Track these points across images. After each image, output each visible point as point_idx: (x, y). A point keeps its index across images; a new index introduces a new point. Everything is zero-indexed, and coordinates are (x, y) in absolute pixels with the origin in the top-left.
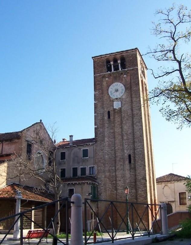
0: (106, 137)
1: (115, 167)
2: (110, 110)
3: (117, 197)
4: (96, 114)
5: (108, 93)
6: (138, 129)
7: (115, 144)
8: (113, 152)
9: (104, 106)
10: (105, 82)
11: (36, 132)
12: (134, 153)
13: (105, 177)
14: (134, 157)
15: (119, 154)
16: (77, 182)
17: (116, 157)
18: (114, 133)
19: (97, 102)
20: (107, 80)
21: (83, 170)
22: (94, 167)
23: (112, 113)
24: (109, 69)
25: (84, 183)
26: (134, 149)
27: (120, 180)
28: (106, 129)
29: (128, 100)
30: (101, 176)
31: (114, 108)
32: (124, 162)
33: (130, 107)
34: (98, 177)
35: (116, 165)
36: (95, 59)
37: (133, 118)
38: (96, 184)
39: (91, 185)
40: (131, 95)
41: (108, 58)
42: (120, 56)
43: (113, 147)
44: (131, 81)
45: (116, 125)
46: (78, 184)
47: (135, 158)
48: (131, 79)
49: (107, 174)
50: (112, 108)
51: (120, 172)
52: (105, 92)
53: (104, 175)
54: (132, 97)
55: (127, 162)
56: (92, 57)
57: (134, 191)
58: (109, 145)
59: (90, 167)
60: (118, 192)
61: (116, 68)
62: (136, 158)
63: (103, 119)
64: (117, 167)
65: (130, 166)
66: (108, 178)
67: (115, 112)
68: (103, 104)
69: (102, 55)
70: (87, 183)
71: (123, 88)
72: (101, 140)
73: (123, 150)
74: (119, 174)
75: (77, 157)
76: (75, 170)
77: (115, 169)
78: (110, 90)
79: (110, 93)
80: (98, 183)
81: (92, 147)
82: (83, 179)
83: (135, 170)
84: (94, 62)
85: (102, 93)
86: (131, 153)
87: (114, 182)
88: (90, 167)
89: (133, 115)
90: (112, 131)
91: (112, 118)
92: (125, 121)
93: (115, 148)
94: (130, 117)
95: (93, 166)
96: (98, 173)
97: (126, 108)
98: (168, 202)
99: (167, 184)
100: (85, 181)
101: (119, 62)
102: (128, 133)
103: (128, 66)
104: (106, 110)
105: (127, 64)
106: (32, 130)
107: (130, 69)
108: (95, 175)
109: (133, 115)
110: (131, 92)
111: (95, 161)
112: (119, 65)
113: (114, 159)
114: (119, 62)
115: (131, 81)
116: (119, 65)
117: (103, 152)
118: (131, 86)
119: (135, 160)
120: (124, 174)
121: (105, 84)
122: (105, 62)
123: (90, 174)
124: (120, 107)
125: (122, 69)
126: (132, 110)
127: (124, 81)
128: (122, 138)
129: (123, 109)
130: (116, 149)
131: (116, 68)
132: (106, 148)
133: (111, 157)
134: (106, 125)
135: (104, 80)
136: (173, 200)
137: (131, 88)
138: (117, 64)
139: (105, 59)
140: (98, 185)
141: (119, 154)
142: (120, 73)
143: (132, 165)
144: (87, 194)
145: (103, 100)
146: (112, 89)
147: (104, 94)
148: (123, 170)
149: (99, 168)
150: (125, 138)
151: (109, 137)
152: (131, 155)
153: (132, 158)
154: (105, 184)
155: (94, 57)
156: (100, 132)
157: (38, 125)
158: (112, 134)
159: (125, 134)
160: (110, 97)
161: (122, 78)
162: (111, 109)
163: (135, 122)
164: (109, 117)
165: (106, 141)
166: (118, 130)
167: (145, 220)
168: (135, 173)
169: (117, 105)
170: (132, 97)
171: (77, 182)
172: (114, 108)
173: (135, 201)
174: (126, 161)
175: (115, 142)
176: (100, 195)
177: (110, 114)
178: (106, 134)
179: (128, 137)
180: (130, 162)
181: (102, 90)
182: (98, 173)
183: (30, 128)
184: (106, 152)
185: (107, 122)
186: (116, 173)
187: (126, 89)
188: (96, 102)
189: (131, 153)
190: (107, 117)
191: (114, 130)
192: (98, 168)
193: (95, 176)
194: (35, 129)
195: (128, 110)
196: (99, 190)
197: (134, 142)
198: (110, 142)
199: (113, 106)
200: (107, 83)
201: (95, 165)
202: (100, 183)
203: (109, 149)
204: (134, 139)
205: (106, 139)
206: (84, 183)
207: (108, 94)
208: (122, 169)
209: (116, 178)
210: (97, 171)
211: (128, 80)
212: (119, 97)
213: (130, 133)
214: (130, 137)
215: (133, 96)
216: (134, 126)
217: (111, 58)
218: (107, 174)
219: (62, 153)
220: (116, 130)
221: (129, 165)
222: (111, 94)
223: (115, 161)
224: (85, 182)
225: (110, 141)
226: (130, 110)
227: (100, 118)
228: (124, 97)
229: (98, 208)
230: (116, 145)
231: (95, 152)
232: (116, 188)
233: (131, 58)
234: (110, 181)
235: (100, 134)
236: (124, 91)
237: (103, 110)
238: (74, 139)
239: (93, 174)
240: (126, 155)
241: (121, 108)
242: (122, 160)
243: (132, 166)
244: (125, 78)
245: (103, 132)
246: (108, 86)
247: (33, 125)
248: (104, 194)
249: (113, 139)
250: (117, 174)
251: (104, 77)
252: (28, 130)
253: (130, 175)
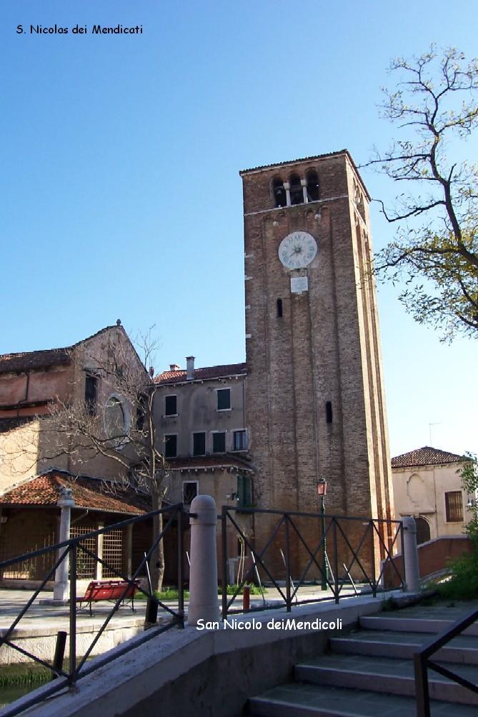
0: (272, 360)
1: (295, 431)
2: (282, 297)
3: (298, 503)
4: (249, 307)
5: (277, 256)
6: (349, 342)
7: (293, 378)
8: (290, 396)
9: (269, 286)
10: (271, 231)
11: (106, 349)
12: (340, 398)
13: (271, 455)
14: (340, 409)
15: (303, 401)
16: (204, 467)
17: (295, 408)
18: (292, 350)
19: (251, 278)
20: (276, 227)
21: (219, 439)
22: (245, 431)
23: (286, 304)
24: (280, 200)
25: (221, 470)
26: (340, 390)
27: (305, 464)
28: (273, 343)
29: (324, 272)
30: (262, 453)
31: (292, 291)
32: (315, 421)
33: (329, 290)
34: (255, 454)
35: (297, 427)
37: (336, 316)
38: (249, 472)
39: (237, 475)
40: (333, 262)
41: (276, 174)
42: (306, 170)
43: (290, 386)
44: (331, 228)
45: (297, 331)
46: (206, 473)
47: (340, 410)
48: (331, 224)
49: (276, 448)
50: (287, 291)
51: (306, 444)
52: (271, 255)
53: (269, 451)
54: (333, 267)
55: (322, 420)
56: (241, 173)
57: (340, 487)
58: (280, 380)
59: (235, 433)
60: (302, 490)
61: (297, 199)
62: (344, 411)
63: (266, 318)
64: (299, 432)
65: (330, 430)
66: (278, 458)
67: (293, 303)
68: (266, 283)
69: (262, 167)
70: (228, 469)
71: (314, 244)
72: (261, 368)
73: (312, 392)
74: (303, 447)
75: (204, 407)
76: (200, 438)
77: (295, 438)
78: (282, 249)
79: (281, 258)
80: (255, 471)
81: (240, 384)
82: (217, 459)
83: (342, 439)
84: (245, 183)
85: (264, 257)
86: (333, 397)
87: (293, 467)
88: (235, 433)
89: (336, 307)
90: (287, 347)
91: (286, 315)
93: (293, 387)
94: (330, 312)
95: (242, 429)
96: (255, 445)
97: (321, 291)
98: (420, 514)
99: (418, 471)
100: (224, 466)
101: (303, 182)
102: (324, 352)
103: (326, 194)
104: (273, 297)
105: (323, 188)
106: (97, 343)
108: (247, 451)
109: (336, 307)
110: (332, 253)
111: (248, 417)
112: (305, 190)
113: (292, 413)
114: (303, 182)
115: (331, 228)
116: (305, 190)
117: (267, 397)
118: (331, 239)
119: (341, 415)
120: (314, 448)
121: (269, 234)
122: (271, 182)
123: (235, 449)
124: (307, 289)
125: (311, 199)
126: (335, 297)
127: (315, 228)
128: (311, 363)
129: (312, 294)
130: (296, 388)
131: (297, 199)
132: (273, 386)
133: (284, 408)
134: (274, 331)
135: (268, 226)
136: (432, 509)
137: (332, 244)
138: (299, 189)
139: (271, 175)
140: (254, 475)
141: (302, 401)
142: (306, 209)
143: (335, 426)
144: (228, 496)
145: (266, 272)
146: (286, 247)
147: (268, 260)
148: (314, 439)
149: (257, 434)
150: (318, 363)
151: (279, 360)
152: (332, 403)
153: (334, 410)
154: (271, 472)
155: (244, 172)
157: (113, 332)
159: (317, 355)
160: (281, 265)
161: (311, 222)
162: (285, 294)
163: (341, 326)
164: (280, 313)
165: (272, 370)
166: (300, 344)
167: (365, 558)
168: (342, 446)
169: (298, 286)
170: (333, 267)
171: (204, 467)
172: (292, 291)
173: (342, 511)
174: (321, 419)
175: (293, 372)
176: (259, 497)
177: (283, 305)
178: (273, 353)
179: (324, 362)
180: (329, 419)
181: (264, 250)
182: (255, 445)
183: (92, 339)
184: (273, 395)
185: (276, 326)
186: (296, 445)
187: (320, 246)
188: (248, 279)
189: (333, 397)
190: (276, 313)
191: (292, 344)
192: (253, 433)
193: (248, 453)
194: (105, 342)
195: (325, 296)
196: (256, 485)
197: (339, 373)
198: (282, 373)
199: (290, 288)
200: (274, 234)
201: (247, 427)
202: (259, 469)
203: (279, 390)
204: (339, 365)
205: (273, 366)
206: (221, 470)
207: (278, 259)
208: (310, 437)
209: (296, 458)
210: (251, 441)
211: (326, 225)
212: (303, 265)
213: (329, 352)
214: (331, 360)
215: (338, 263)
217: (285, 175)
218: (276, 448)
219: (168, 398)
220: (295, 345)
221: (326, 428)
222: (285, 259)
223: (295, 417)
224: (224, 468)
225: (283, 371)
226: (330, 297)
227: (258, 315)
228: (314, 266)
229: (253, 528)
230: (296, 380)
231: (247, 395)
232: (297, 482)
233: (331, 173)
234: (282, 465)
235: (259, 353)
236: (315, 252)
237: (266, 297)
238: (198, 365)
239: (241, 448)
240: (321, 403)
241: (307, 293)
242: (311, 416)
243: (335, 429)
244: (317, 220)
245: (267, 349)
246: (278, 241)
247: (99, 332)
248: (268, 495)
249: (290, 365)
250: (299, 448)
251: (268, 218)
252: (88, 344)
253: (331, 450)
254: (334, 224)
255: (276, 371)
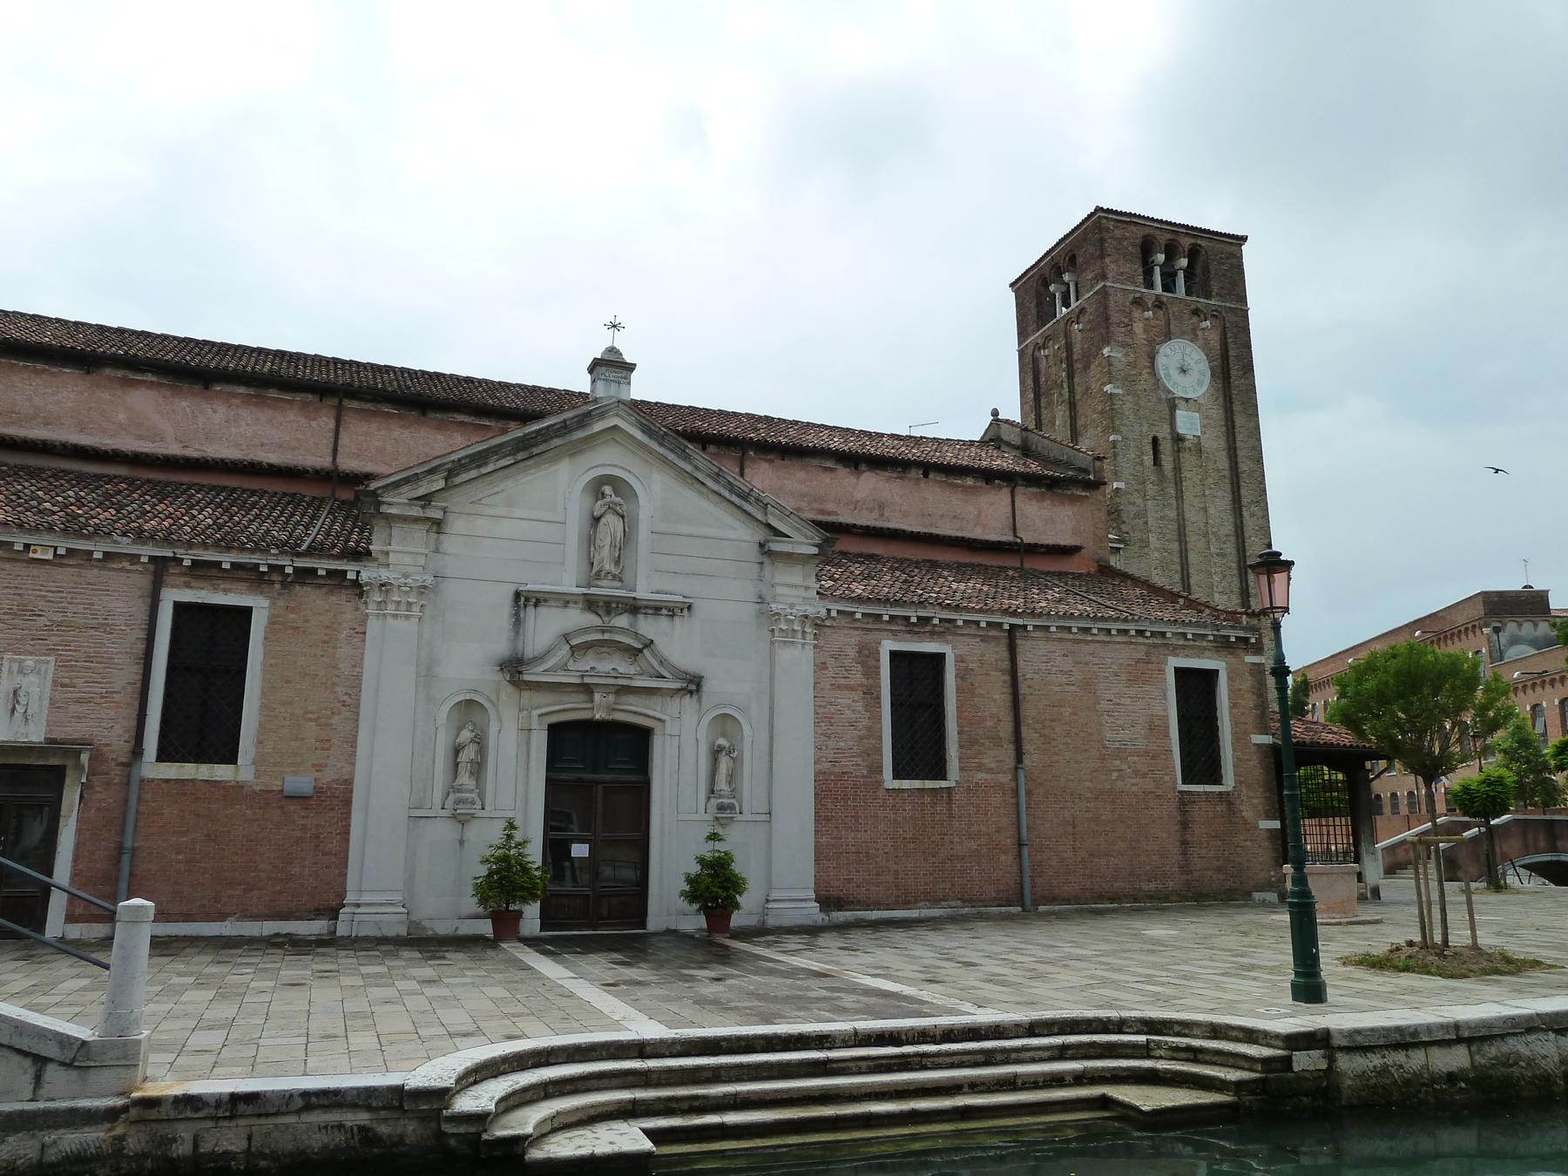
6: (1257, 528)
10: (1141, 324)
20: (1147, 319)
23: (1166, 447)
36: (1106, 218)
61: (1169, 286)
92: (1211, 488)
107: (1223, 304)
131: (1169, 286)
134: (1151, 486)
156: (1135, 509)
158: (1170, 526)
162: (1163, 433)
179: (1221, 549)
185: (1153, 478)
195: (1217, 450)
211: (1214, 338)
216: (1246, 514)
254: (1231, 346)
255: (1157, 549)
